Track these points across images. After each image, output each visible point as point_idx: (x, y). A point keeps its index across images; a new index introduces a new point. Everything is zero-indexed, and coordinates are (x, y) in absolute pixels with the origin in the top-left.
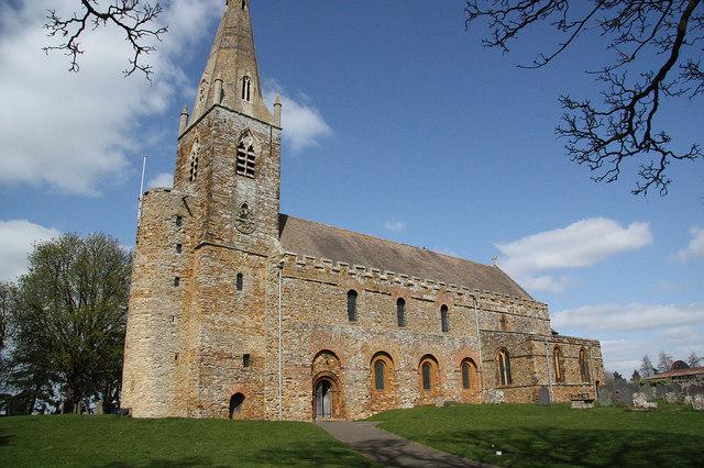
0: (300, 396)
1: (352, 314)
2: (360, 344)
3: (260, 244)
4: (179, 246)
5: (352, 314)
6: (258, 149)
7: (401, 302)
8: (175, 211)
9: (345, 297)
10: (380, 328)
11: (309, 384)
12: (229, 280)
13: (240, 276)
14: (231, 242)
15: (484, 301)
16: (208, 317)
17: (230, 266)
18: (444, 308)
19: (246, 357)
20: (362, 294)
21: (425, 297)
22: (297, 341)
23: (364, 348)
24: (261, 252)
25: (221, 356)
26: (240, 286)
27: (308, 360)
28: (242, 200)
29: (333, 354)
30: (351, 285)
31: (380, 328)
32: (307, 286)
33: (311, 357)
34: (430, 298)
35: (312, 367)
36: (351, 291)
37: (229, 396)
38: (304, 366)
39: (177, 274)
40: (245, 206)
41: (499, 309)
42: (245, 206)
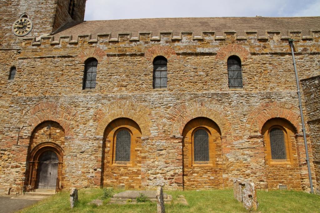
0: (12, 167)
2: (92, 111)
7: (160, 62)
10: (125, 93)
11: (23, 156)
14: (9, 45)
15: (308, 43)
18: (234, 60)
20: (103, 61)
21: (199, 50)
22: (18, 115)
27: (27, 132)
29: (56, 125)
31: (125, 93)
32: (39, 63)
33: (31, 129)
34: (207, 50)
35: (32, 137)
38: (21, 137)
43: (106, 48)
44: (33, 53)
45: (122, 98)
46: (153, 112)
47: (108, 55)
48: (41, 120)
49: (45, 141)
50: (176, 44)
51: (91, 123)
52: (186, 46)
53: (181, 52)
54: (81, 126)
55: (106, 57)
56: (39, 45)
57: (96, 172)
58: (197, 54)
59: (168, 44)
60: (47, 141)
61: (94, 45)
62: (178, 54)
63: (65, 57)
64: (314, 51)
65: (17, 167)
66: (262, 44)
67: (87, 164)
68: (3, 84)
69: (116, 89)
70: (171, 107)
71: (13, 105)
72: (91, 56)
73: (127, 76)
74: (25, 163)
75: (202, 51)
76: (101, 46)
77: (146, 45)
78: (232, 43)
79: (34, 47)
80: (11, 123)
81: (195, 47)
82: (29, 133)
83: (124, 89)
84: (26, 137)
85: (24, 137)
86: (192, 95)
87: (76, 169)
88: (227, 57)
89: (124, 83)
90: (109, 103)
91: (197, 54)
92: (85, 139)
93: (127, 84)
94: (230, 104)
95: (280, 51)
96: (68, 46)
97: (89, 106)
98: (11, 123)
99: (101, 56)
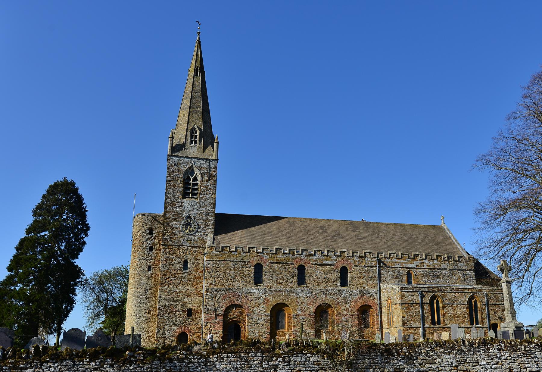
1: (258, 280)
2: (261, 299)
3: (200, 240)
4: (151, 249)
5: (258, 280)
6: (199, 178)
8: (148, 227)
9: (252, 269)
12: (176, 264)
13: (186, 262)
14: (179, 241)
16: (163, 288)
17: (178, 256)
19: (189, 312)
21: (325, 262)
22: (213, 300)
23: (266, 301)
24: (199, 246)
25: (172, 311)
26: (185, 266)
27: (221, 312)
28: (185, 215)
30: (256, 260)
32: (222, 265)
34: (329, 262)
36: (257, 264)
37: (176, 334)
39: (149, 264)
40: (189, 217)
41: (405, 265)
42: (189, 217)
43: (268, 257)
44: (216, 257)
45: (280, 291)
46: (298, 300)
47: (271, 263)
48: (230, 303)
49: (233, 317)
50: (311, 257)
51: (262, 306)
52: (317, 259)
53: (314, 263)
54: (256, 308)
55: (268, 264)
56: (220, 251)
57: (267, 335)
58: (323, 265)
59: (306, 257)
60: (234, 317)
61: (259, 254)
62: (313, 264)
63: (241, 262)
64: (390, 265)
65: (216, 333)
66: (361, 259)
67: (261, 330)
68: (180, 273)
69: (275, 285)
70: (309, 297)
71: (208, 293)
72: (258, 262)
73: (282, 277)
74: (222, 330)
75: (326, 263)
76: (265, 256)
77: (293, 257)
78: (344, 258)
79: (217, 252)
80: (208, 305)
81: (322, 260)
82: (222, 312)
83: (280, 285)
84: (221, 314)
85: (219, 315)
86: (320, 290)
87: (255, 333)
88: (340, 267)
89: (281, 281)
90: (272, 293)
91: (323, 265)
92: (259, 315)
93: (282, 282)
94: (341, 296)
95: (370, 265)
96: (242, 253)
97: (260, 295)
98: (208, 305)
99: (265, 263)
